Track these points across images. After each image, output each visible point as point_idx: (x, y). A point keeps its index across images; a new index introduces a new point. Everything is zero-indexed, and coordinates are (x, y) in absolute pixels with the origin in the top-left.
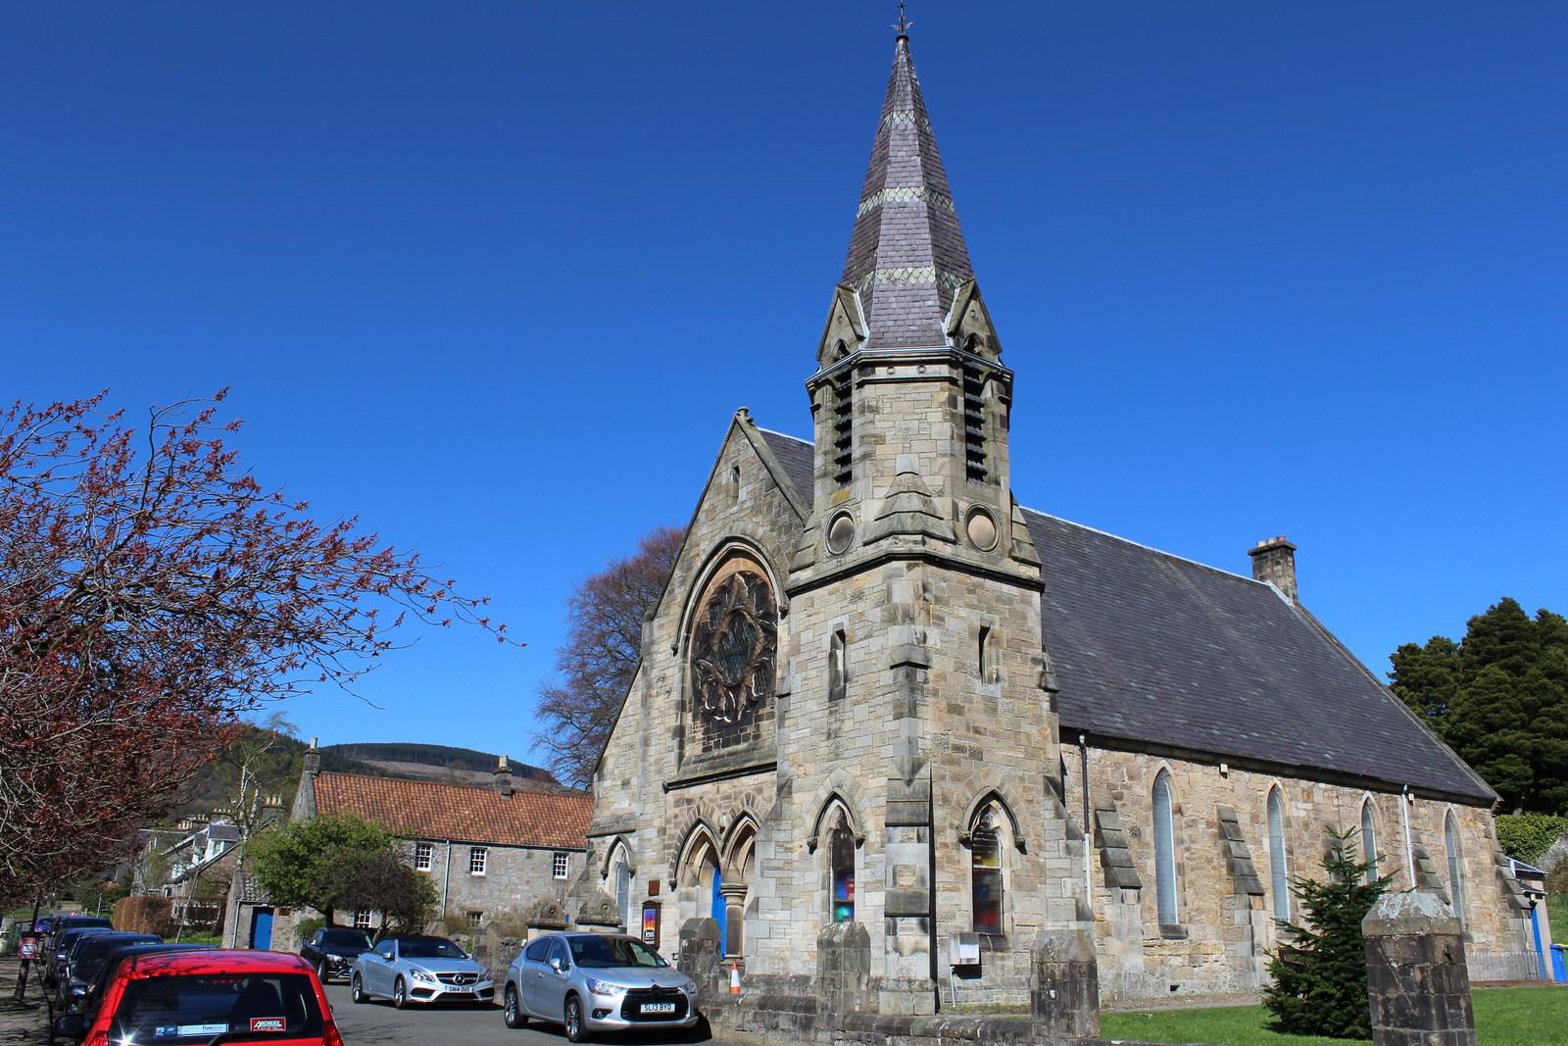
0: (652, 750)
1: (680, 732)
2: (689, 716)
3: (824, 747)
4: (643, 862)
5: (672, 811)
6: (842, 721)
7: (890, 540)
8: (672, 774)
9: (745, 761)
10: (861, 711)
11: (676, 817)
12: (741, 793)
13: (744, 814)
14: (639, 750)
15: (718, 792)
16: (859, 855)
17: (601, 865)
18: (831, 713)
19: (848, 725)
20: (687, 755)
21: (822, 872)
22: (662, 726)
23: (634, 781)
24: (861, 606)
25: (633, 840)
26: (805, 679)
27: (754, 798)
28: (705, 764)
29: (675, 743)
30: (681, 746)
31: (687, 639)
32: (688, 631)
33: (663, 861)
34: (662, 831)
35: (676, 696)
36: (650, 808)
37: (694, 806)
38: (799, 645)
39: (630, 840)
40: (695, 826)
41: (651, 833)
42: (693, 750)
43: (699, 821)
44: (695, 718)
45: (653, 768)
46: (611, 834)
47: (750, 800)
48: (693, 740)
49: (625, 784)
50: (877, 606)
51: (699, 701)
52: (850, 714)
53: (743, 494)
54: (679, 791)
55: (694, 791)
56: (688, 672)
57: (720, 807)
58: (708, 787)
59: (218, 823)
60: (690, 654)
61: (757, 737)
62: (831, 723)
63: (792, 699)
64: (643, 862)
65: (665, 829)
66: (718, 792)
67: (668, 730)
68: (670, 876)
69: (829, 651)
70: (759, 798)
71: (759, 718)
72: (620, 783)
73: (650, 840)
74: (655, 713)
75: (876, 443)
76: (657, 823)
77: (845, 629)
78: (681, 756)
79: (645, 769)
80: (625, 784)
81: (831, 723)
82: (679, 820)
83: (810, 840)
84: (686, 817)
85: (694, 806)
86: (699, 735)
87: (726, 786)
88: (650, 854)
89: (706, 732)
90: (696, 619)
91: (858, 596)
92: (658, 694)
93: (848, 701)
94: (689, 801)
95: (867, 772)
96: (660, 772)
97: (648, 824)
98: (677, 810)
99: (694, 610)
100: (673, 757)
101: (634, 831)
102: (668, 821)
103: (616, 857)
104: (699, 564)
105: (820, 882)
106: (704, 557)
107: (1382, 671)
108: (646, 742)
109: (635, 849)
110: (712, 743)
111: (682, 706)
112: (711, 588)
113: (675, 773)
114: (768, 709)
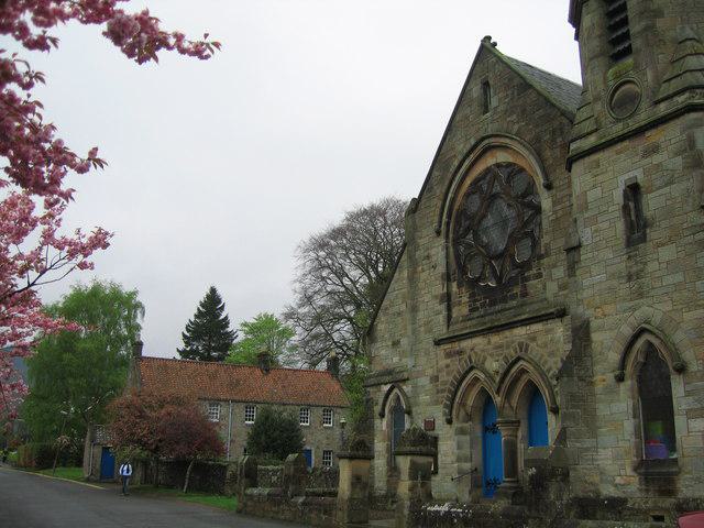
0: (421, 315)
1: (447, 298)
2: (454, 285)
3: (624, 288)
4: (417, 405)
5: (443, 362)
6: (646, 263)
7: (687, 95)
8: (441, 330)
9: (515, 316)
10: (667, 253)
11: (447, 366)
12: (513, 342)
13: (519, 359)
14: (408, 316)
15: (489, 342)
16: (678, 388)
17: (377, 409)
18: (629, 257)
19: (652, 267)
20: (454, 316)
21: (631, 403)
22: (429, 296)
23: (404, 342)
24: (656, 159)
25: (407, 388)
26: (596, 231)
27: (527, 346)
28: (474, 322)
29: (443, 307)
30: (449, 309)
31: (448, 224)
32: (449, 216)
33: (436, 403)
34: (435, 379)
35: (441, 269)
36: (422, 360)
37: (466, 356)
38: (586, 203)
39: (404, 387)
40: (467, 372)
41: (424, 381)
42: (460, 311)
43: (472, 368)
44: (459, 286)
45: (422, 329)
46: (386, 384)
47: (523, 347)
48: (460, 303)
49: (396, 344)
50: (677, 154)
51: (462, 269)
52: (655, 256)
53: (494, 102)
54: (449, 346)
55: (466, 344)
56: (451, 250)
57: (492, 355)
58: (478, 341)
59: (433, 509)
60: (451, 236)
61: (525, 294)
62: (631, 267)
63: (582, 251)
64: (417, 405)
65: (437, 377)
66: (489, 342)
67: (436, 297)
68: (445, 414)
69: (622, 203)
70: (533, 345)
71: (527, 279)
72: (390, 343)
73: (423, 386)
74: (421, 285)
75: (655, 16)
76: (430, 372)
77: (639, 181)
78: (449, 317)
79: (414, 331)
80: (396, 344)
81: (631, 267)
82: (451, 368)
83: (618, 372)
84: (457, 366)
85: (466, 356)
86: (465, 299)
87: (495, 339)
88: (424, 398)
89: (472, 296)
90: (456, 207)
91: (655, 149)
92: (423, 271)
93: (650, 245)
94: (460, 353)
95: (680, 307)
96: (430, 331)
97: (421, 374)
98: (449, 361)
99: (453, 200)
100: (441, 318)
101: (408, 379)
102: (439, 371)
103: (391, 402)
104: (456, 163)
105: (630, 411)
106: (460, 157)
107: (178, 357)
108: (414, 309)
109: (409, 395)
110: (478, 304)
111: (448, 278)
112: (468, 181)
113: (445, 331)
114: (534, 271)
